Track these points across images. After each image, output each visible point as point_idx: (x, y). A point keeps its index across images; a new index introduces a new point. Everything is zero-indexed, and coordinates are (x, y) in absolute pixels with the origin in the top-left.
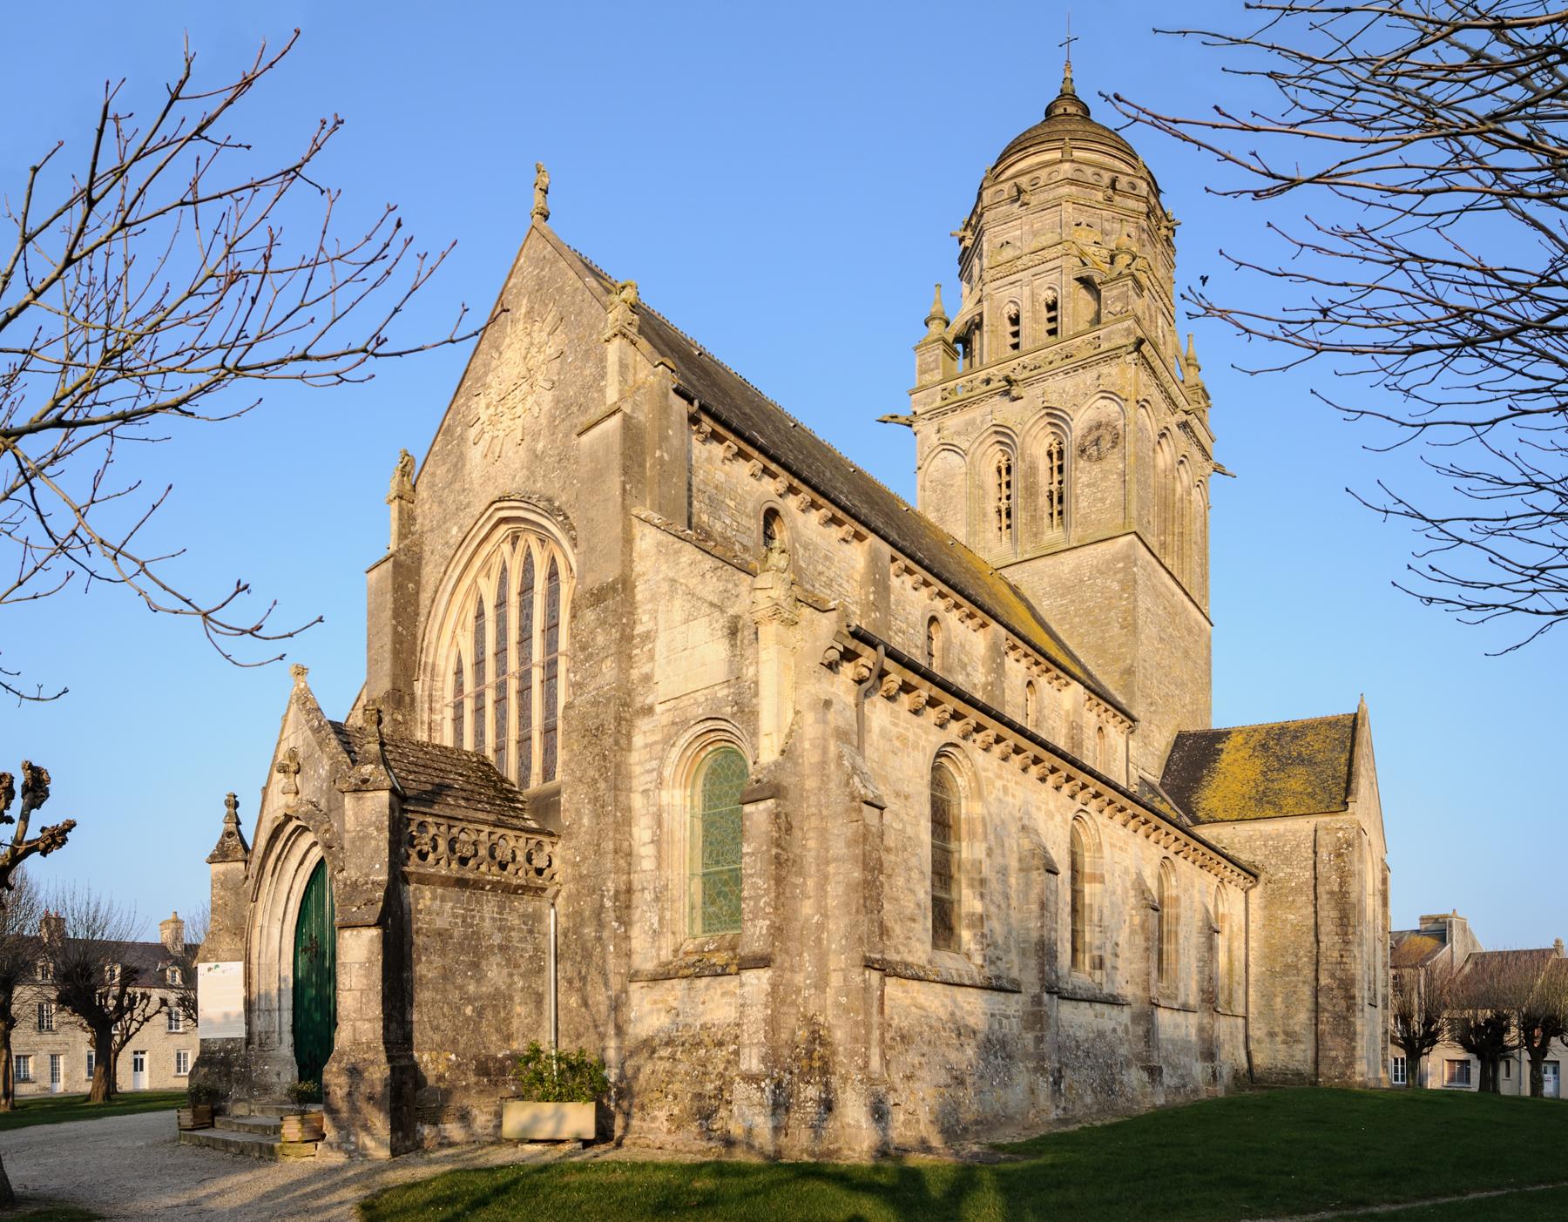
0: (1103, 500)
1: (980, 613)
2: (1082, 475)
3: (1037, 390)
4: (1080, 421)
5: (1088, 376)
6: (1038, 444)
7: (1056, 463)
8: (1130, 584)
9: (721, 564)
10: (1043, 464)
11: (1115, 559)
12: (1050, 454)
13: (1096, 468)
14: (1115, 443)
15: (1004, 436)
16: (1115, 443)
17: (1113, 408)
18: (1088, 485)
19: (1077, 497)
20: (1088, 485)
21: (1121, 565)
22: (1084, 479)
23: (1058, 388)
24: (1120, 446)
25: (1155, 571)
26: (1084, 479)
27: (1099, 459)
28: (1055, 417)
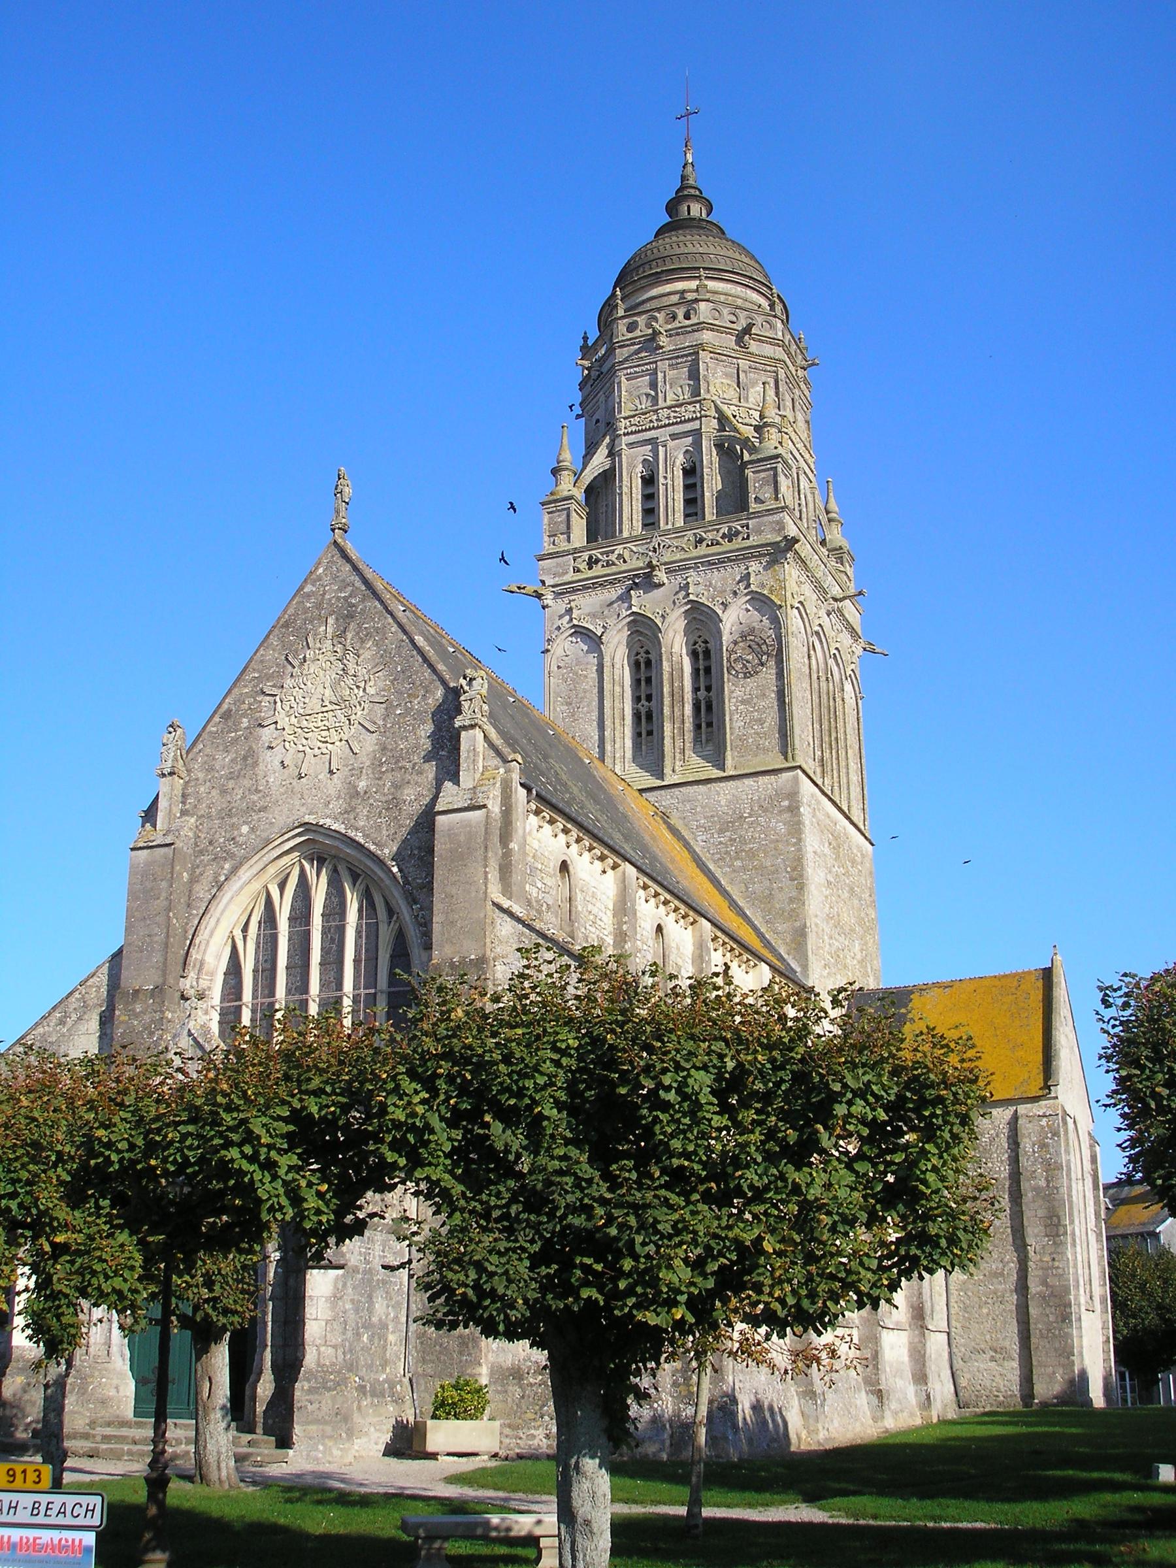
0: (761, 722)
1: (691, 913)
7: (702, 664)
15: (644, 634)
18: (743, 702)
21: (786, 803)
25: (818, 802)
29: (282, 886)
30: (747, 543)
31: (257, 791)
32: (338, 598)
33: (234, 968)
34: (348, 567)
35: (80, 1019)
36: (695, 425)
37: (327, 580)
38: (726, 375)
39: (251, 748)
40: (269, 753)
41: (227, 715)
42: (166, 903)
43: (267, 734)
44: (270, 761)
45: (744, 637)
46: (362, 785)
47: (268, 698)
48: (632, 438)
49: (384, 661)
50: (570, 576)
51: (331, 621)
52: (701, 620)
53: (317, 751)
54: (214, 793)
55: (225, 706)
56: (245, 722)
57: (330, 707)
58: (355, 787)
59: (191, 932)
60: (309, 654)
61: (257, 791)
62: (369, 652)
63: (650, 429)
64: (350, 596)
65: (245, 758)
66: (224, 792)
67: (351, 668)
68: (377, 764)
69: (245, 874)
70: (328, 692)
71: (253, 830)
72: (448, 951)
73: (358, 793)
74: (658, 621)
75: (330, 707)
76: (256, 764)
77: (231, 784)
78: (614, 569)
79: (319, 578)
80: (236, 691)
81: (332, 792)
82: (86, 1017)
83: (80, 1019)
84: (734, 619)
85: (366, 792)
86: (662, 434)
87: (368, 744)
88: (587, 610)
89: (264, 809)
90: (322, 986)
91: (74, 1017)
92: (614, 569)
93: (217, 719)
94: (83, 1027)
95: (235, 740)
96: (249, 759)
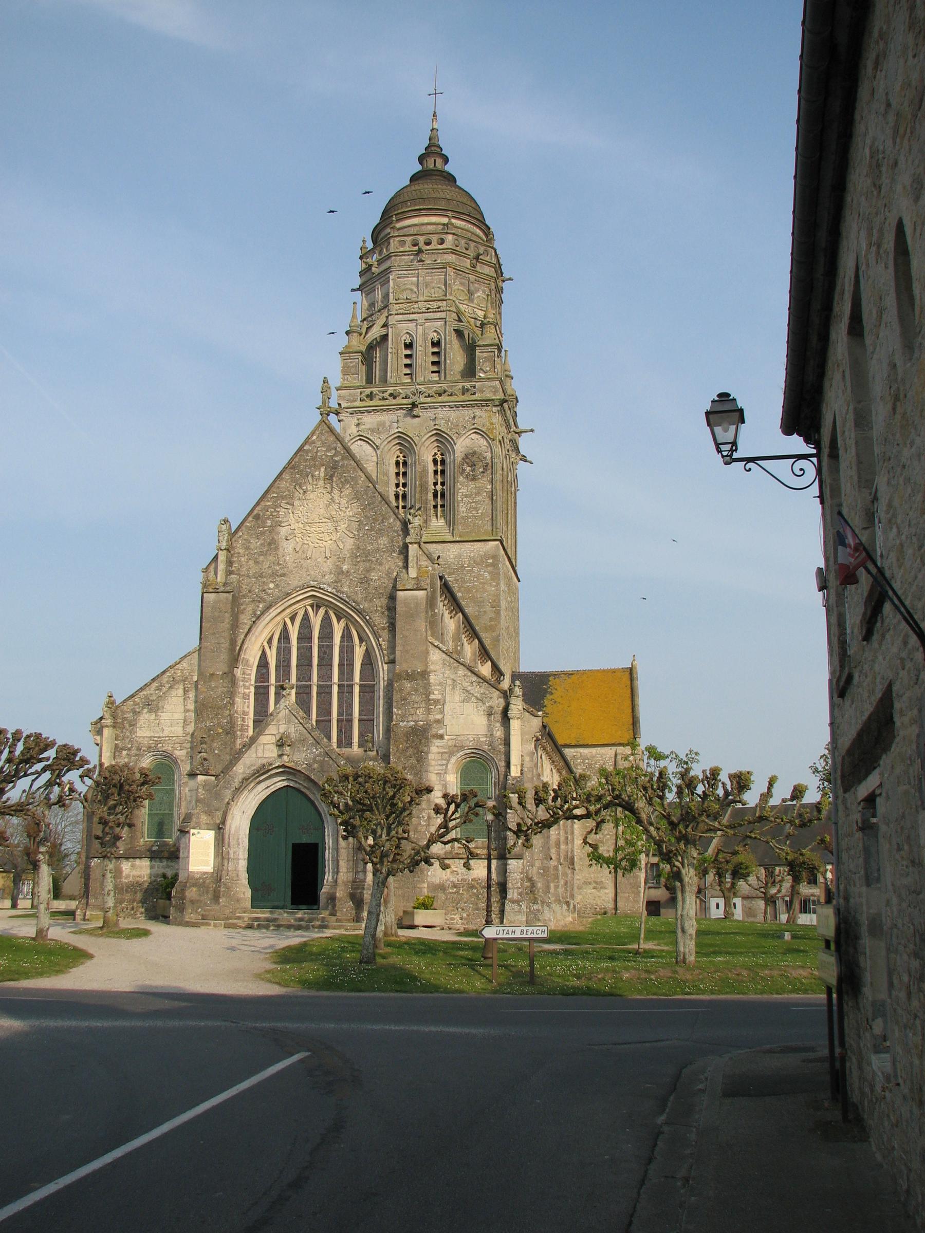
0: (476, 509)
2: (463, 489)
3: (430, 414)
4: (462, 445)
5: (467, 413)
6: (427, 453)
7: (440, 468)
8: (495, 576)
9: (469, 674)
10: (431, 468)
11: (486, 556)
12: (435, 462)
13: (472, 485)
14: (485, 469)
15: (405, 443)
16: (485, 469)
17: (483, 442)
18: (466, 496)
19: (458, 503)
20: (466, 496)
22: (463, 490)
23: (446, 417)
24: (489, 471)
26: (463, 490)
27: (474, 479)
28: (442, 439)
29: (293, 619)
30: (474, 397)
31: (279, 564)
32: (327, 456)
33: (263, 663)
34: (332, 438)
35: (171, 687)
36: (443, 315)
37: (319, 444)
38: (461, 284)
39: (273, 538)
40: (286, 542)
41: (257, 517)
43: (283, 531)
44: (287, 548)
45: (467, 456)
46: (345, 567)
48: (400, 317)
49: (357, 497)
52: (442, 439)
53: (316, 545)
54: (251, 563)
55: (256, 512)
56: (269, 523)
57: (324, 520)
59: (239, 642)
60: (310, 488)
61: (279, 564)
62: (347, 491)
64: (334, 455)
65: (270, 544)
66: (256, 562)
67: (336, 497)
68: (354, 556)
69: (273, 612)
70: (322, 511)
71: (277, 586)
72: (405, 666)
74: (416, 439)
75: (324, 520)
76: (277, 548)
77: (262, 558)
78: (387, 402)
79: (314, 442)
80: (262, 503)
81: (327, 570)
83: (171, 687)
84: (462, 445)
87: (350, 543)
88: (368, 426)
89: (284, 575)
90: (319, 677)
91: (167, 686)
92: (387, 402)
93: (250, 519)
95: (263, 533)
96: (272, 545)
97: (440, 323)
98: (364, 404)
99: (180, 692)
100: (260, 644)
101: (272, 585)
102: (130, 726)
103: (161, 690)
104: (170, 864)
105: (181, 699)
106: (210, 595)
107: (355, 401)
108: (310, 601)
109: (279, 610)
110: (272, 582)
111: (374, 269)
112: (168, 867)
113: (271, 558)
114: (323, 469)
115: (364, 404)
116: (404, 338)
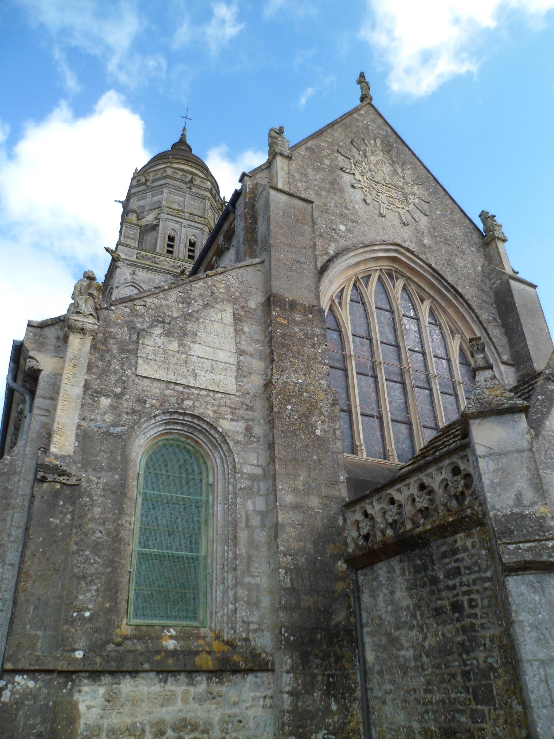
31: (346, 208)
36: (202, 226)
39: (335, 179)
40: (351, 190)
42: (311, 244)
46: (426, 241)
47: (342, 157)
50: (134, 259)
51: (378, 141)
58: (422, 241)
61: (346, 208)
63: (181, 218)
65: (331, 183)
67: (399, 171)
69: (350, 259)
70: (387, 178)
71: (349, 231)
73: (425, 246)
82: (218, 306)
83: (206, 305)
85: (429, 247)
86: (185, 223)
91: (200, 302)
94: (214, 315)
97: (197, 231)
98: (138, 261)
99: (228, 317)
100: (330, 296)
101: (342, 228)
102: (122, 350)
103: (189, 305)
104: (216, 688)
105: (232, 330)
106: (279, 195)
107: (132, 256)
108: (386, 265)
109: (357, 259)
110: (341, 223)
111: (148, 184)
112: (212, 697)
113: (336, 198)
114: (378, 141)
115: (138, 261)
116: (169, 232)
